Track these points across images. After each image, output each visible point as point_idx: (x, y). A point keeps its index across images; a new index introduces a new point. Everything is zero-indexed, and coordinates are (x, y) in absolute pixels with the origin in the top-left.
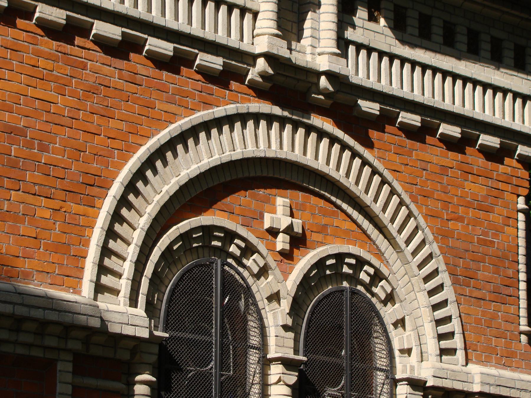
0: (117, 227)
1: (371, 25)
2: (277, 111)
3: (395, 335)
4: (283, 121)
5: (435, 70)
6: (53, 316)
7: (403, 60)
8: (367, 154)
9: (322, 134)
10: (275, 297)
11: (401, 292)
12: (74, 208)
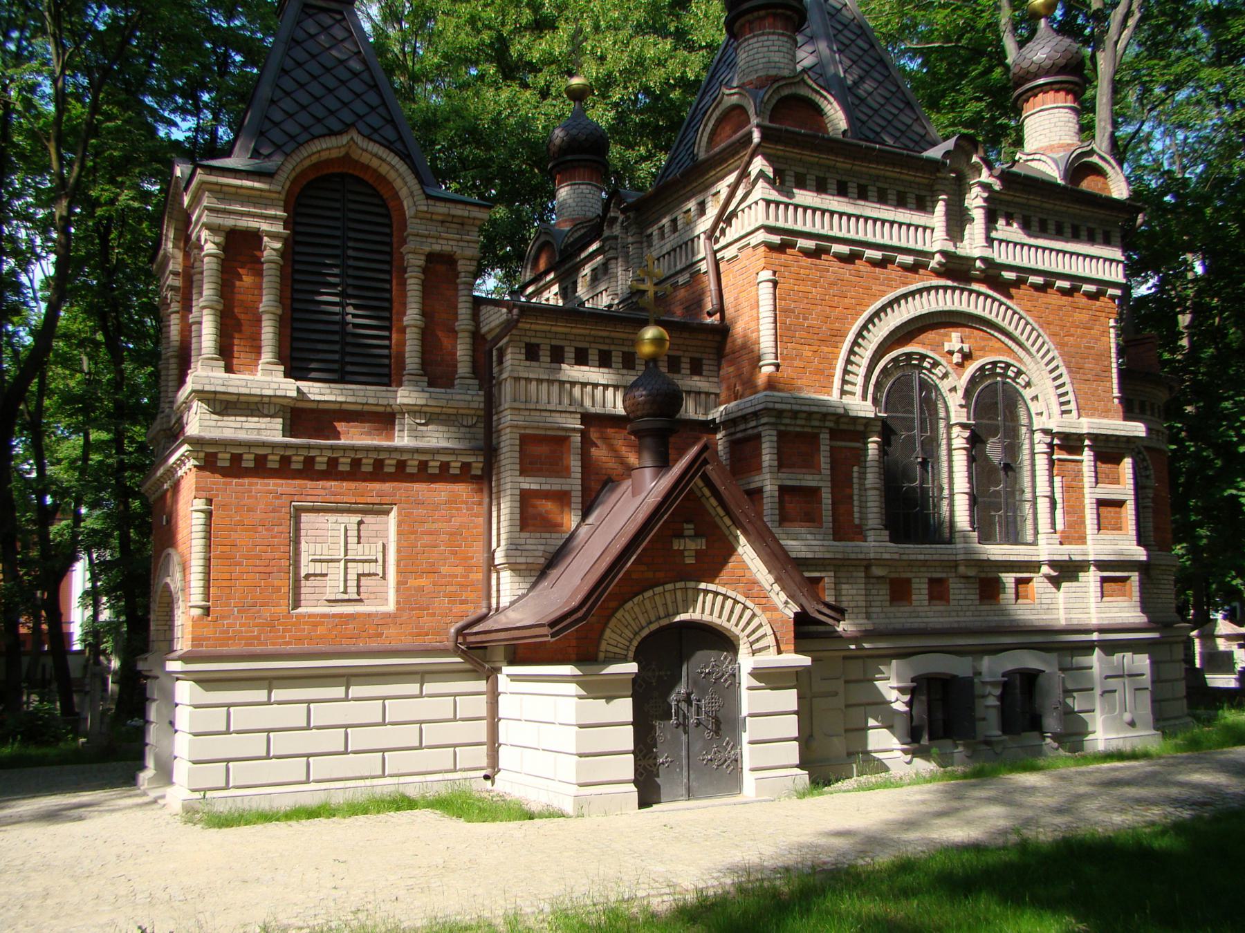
0: (852, 358)
1: (1008, 228)
2: (949, 283)
3: (1034, 407)
4: (953, 289)
5: (1051, 250)
6: (815, 409)
7: (1030, 246)
8: (1009, 302)
9: (979, 294)
10: (954, 389)
11: (1034, 380)
12: (826, 349)
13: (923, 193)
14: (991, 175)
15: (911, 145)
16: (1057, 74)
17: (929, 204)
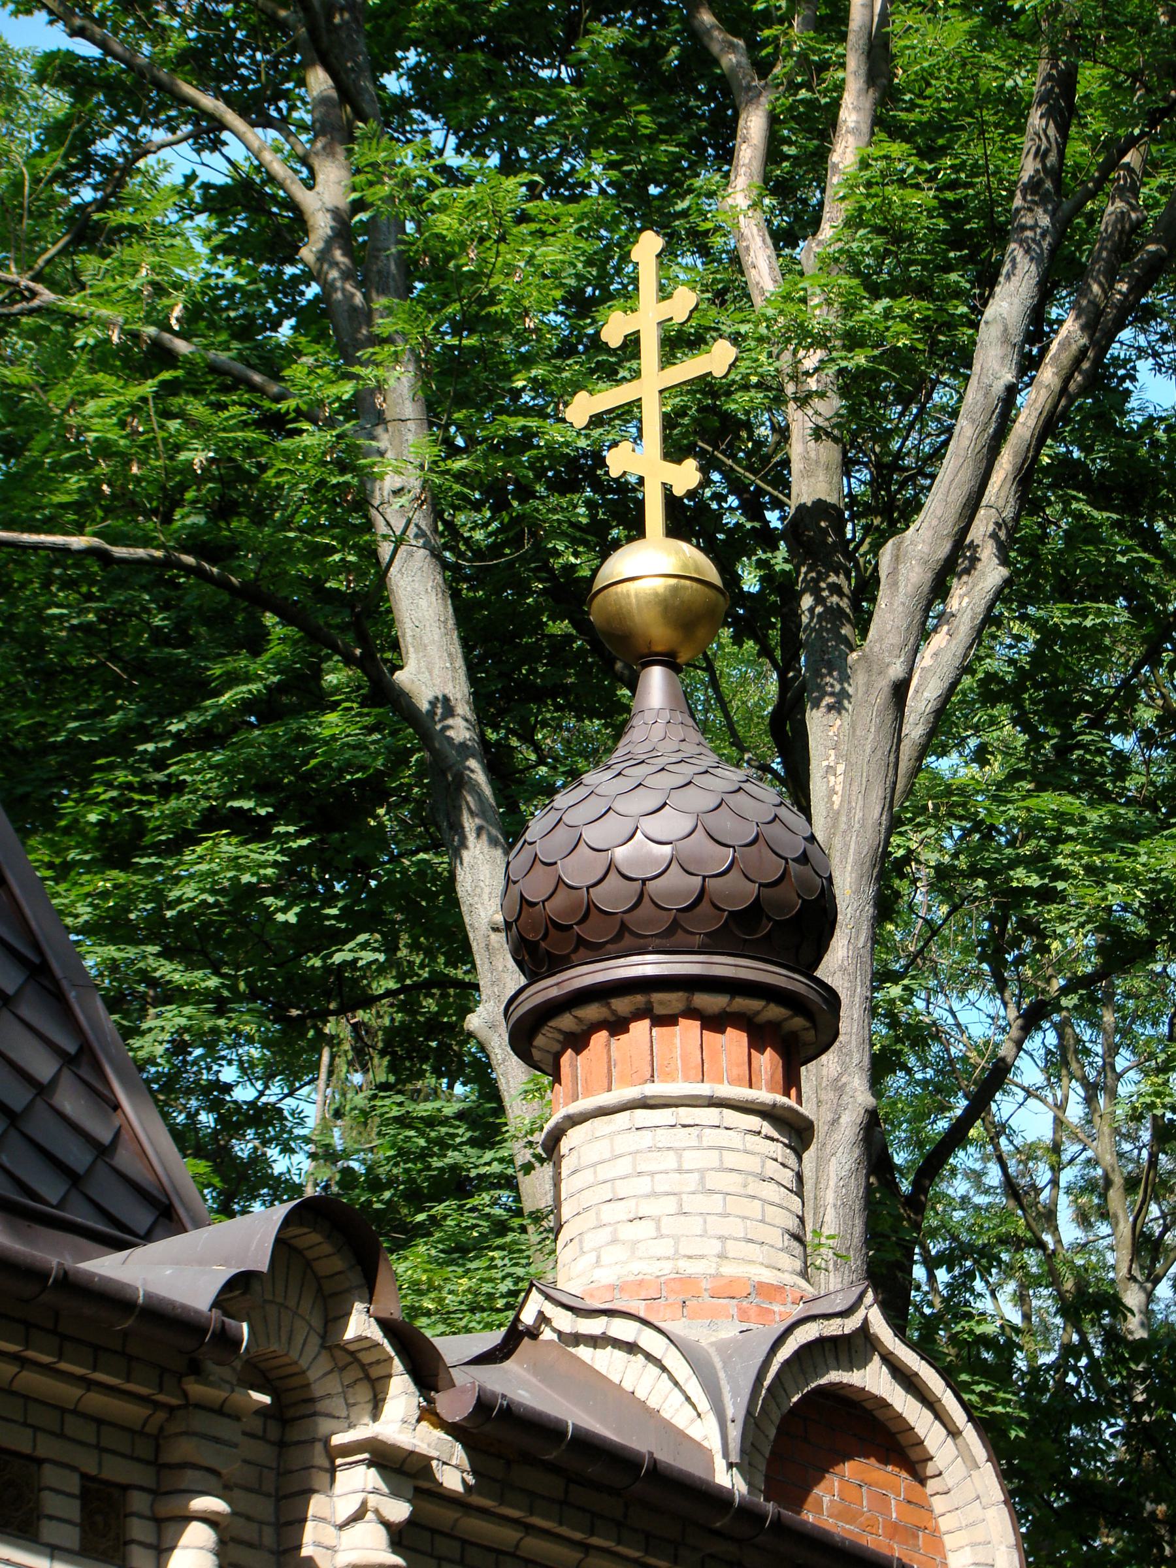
13: (117, 1471)
14: (428, 1414)
15: (51, 1189)
16: (711, 946)
17: (139, 1529)
